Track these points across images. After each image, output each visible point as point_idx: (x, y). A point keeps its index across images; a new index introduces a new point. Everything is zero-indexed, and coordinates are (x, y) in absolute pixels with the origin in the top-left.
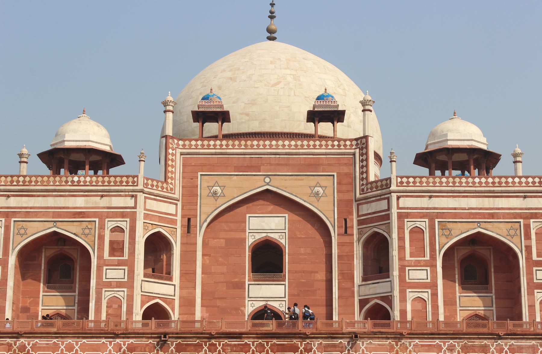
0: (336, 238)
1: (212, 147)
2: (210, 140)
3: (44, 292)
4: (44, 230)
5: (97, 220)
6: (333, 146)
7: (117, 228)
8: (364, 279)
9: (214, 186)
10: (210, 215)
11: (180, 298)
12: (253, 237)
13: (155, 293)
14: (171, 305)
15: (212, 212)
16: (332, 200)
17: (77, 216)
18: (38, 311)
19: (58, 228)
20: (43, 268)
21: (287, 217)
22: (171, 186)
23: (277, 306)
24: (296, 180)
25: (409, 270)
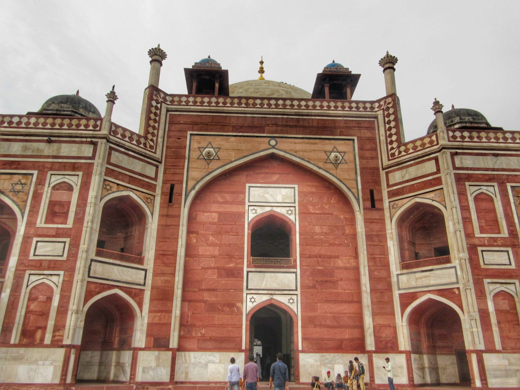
2: (204, 97)
5: (35, 173)
6: (351, 108)
7: (63, 185)
9: (207, 147)
10: (200, 181)
11: (153, 288)
12: (254, 211)
13: (112, 280)
14: (138, 299)
15: (203, 178)
16: (354, 167)
17: (8, 166)
21: (297, 188)
22: (152, 143)
24: (308, 143)
25: (482, 251)
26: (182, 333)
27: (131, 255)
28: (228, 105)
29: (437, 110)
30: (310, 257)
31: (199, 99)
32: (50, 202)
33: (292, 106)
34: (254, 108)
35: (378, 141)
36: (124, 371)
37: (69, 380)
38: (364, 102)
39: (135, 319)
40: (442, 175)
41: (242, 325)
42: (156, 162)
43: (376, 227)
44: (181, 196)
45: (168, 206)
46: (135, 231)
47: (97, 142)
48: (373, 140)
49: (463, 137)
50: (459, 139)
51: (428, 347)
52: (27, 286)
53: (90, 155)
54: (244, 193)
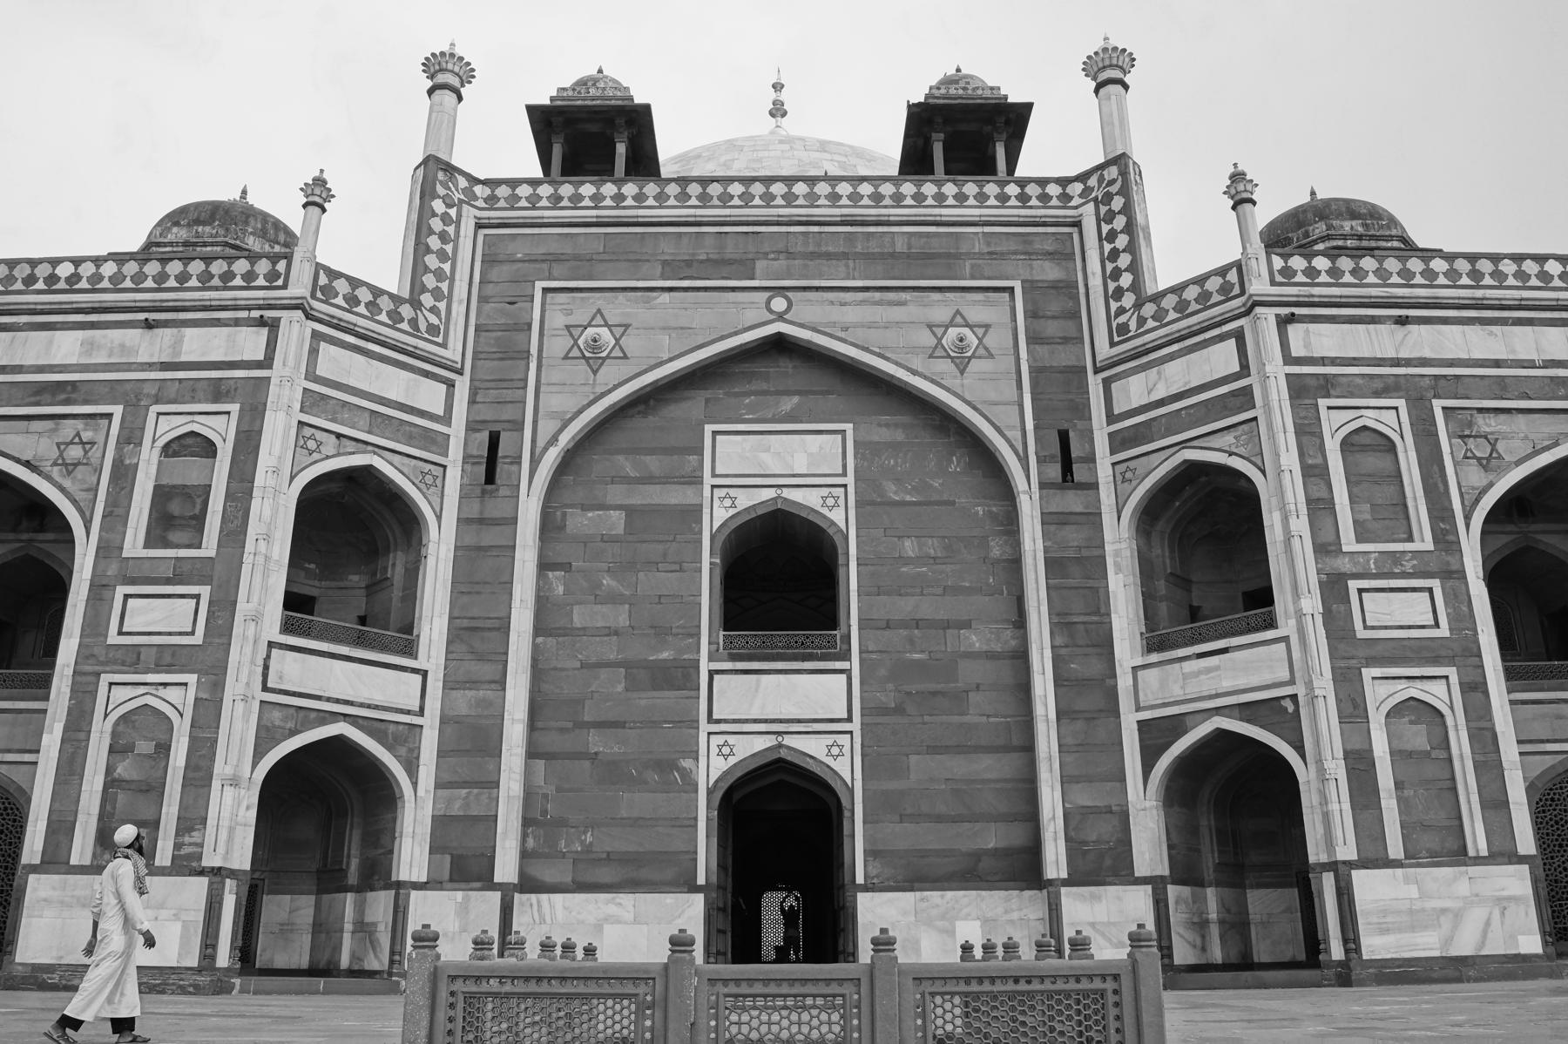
0: (1036, 496)
1: (587, 202)
2: (583, 183)
5: (117, 410)
6: (1002, 198)
7: (189, 441)
9: (589, 325)
11: (444, 720)
12: (728, 502)
13: (329, 700)
14: (403, 751)
15: (580, 412)
17: (47, 397)
22: (434, 320)
23: (821, 754)
24: (879, 303)
25: (1360, 591)
26: (531, 843)
27: (384, 628)
28: (651, 202)
29: (1238, 197)
30: (888, 627)
31: (566, 190)
32: (158, 489)
33: (834, 197)
34: (724, 207)
36: (374, 944)
37: (223, 958)
38: (1042, 182)
41: (696, 819)
42: (444, 373)
43: (1074, 536)
45: (484, 492)
46: (396, 566)
48: (1067, 288)
49: (1311, 272)
50: (1300, 278)
51: (1219, 867)
52: (106, 715)
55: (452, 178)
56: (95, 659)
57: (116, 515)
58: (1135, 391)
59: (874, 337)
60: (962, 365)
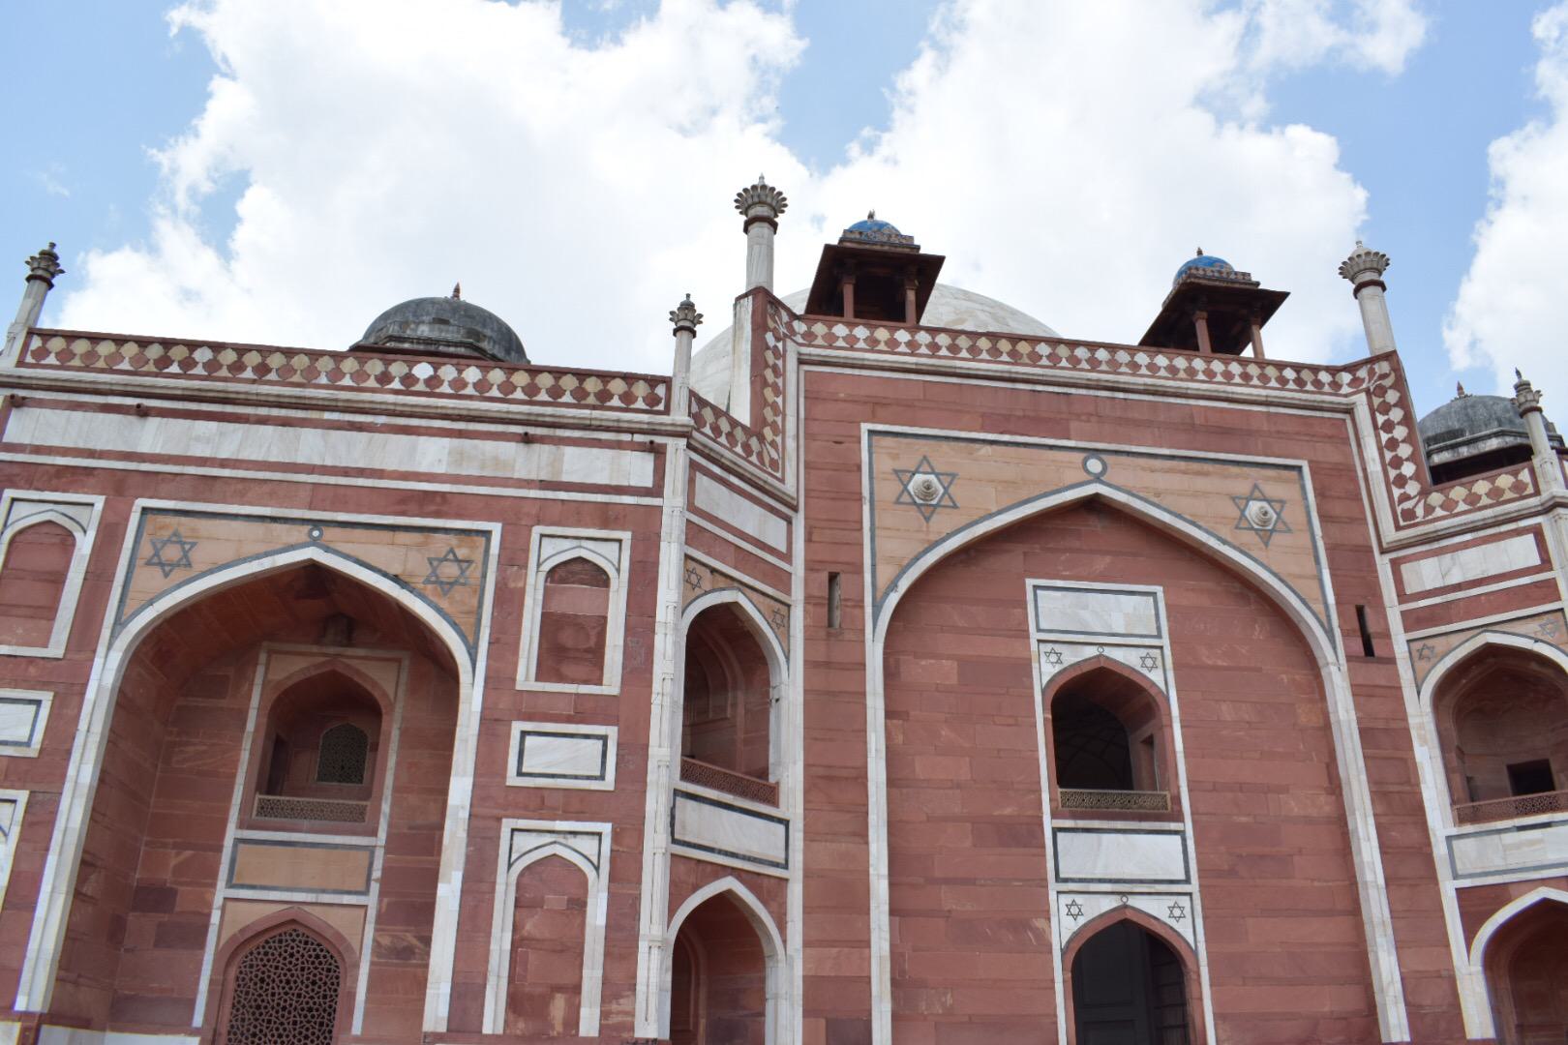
0: (1344, 667)
3: (241, 825)
4: (267, 554)
7: (577, 567)
8: (1462, 819)
11: (808, 875)
13: (720, 852)
15: (917, 558)
16: (1309, 544)
18: (209, 905)
19: (327, 549)
20: (250, 726)
22: (774, 455)
23: (1163, 915)
30: (1214, 790)
35: (1360, 474)
39: (769, 964)
40: (1556, 574)
41: (1053, 981)
44: (862, 607)
45: (829, 634)
47: (664, 446)
52: (510, 865)
53: (649, 483)
54: (1023, 605)
55: (777, 312)
56: (497, 802)
57: (505, 644)
58: (1427, 574)
59: (1184, 504)
60: (1265, 534)
